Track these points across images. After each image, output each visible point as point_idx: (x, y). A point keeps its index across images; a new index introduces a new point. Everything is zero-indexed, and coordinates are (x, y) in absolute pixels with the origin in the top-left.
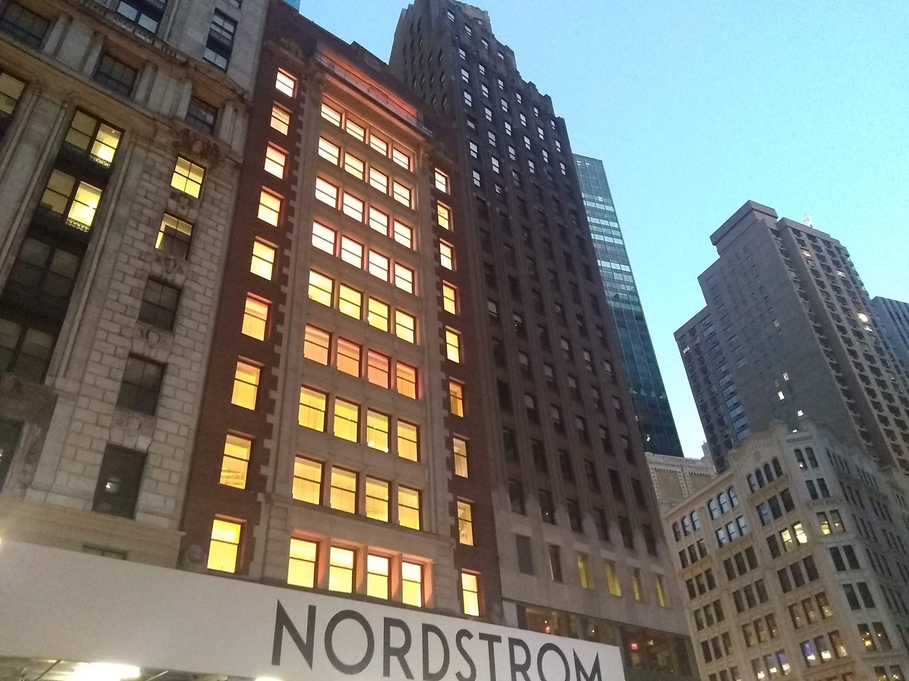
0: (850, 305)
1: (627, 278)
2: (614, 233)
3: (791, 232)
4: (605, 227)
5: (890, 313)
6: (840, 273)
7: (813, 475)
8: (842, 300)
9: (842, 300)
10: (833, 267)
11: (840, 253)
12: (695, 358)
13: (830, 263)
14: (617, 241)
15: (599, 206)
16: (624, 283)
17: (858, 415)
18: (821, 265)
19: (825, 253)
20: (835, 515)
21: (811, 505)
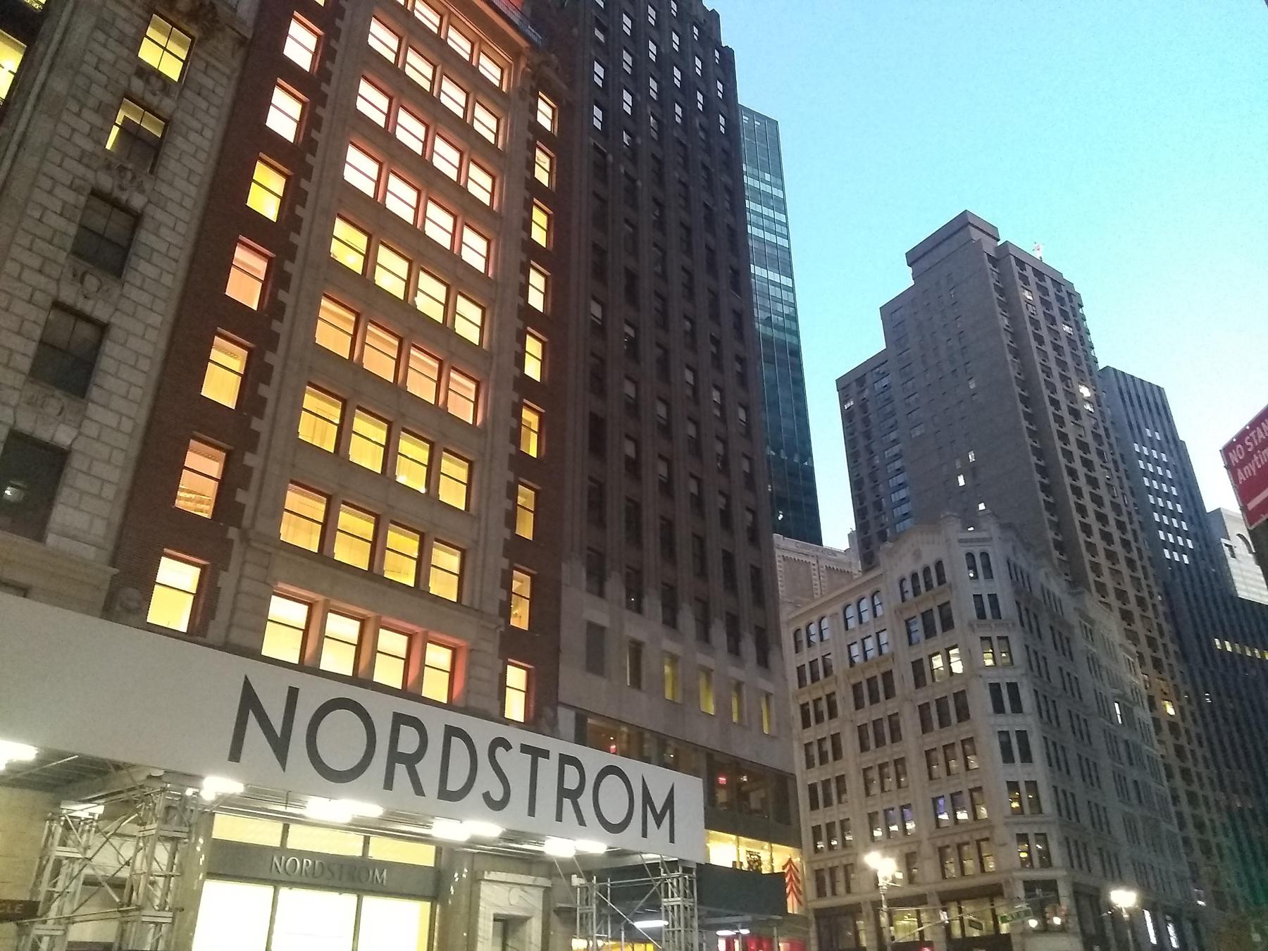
0: (1071, 374)
1: (786, 296)
3: (1013, 262)
4: (768, 218)
5: (1120, 389)
6: (1066, 328)
7: (984, 588)
8: (1062, 364)
9: (1062, 364)
10: (1059, 318)
11: (1071, 301)
12: (858, 417)
13: (1056, 312)
14: (782, 242)
15: (764, 187)
16: (781, 301)
17: (1055, 519)
18: (1044, 313)
19: (1052, 298)
20: (1004, 642)
21: (975, 627)
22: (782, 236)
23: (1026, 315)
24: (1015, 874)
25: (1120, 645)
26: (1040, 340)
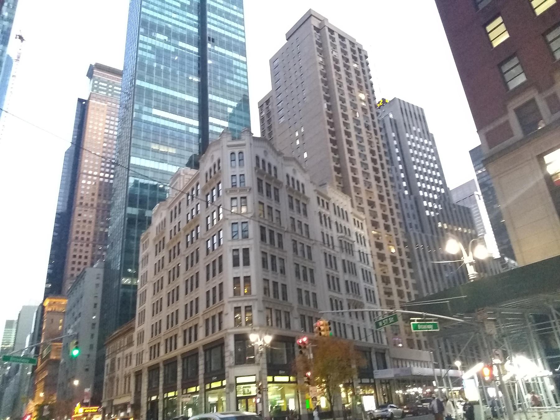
0: (355, 86)
1: (242, 65)
2: (240, 32)
3: (327, 30)
5: (401, 108)
6: (355, 65)
8: (350, 82)
9: (350, 82)
10: (351, 60)
11: (360, 53)
12: (266, 119)
13: (349, 56)
15: (233, 12)
17: (337, 156)
18: (343, 57)
19: (348, 49)
20: (261, 206)
22: (241, 36)
23: (331, 56)
24: (229, 331)
25: (352, 213)
26: (338, 69)
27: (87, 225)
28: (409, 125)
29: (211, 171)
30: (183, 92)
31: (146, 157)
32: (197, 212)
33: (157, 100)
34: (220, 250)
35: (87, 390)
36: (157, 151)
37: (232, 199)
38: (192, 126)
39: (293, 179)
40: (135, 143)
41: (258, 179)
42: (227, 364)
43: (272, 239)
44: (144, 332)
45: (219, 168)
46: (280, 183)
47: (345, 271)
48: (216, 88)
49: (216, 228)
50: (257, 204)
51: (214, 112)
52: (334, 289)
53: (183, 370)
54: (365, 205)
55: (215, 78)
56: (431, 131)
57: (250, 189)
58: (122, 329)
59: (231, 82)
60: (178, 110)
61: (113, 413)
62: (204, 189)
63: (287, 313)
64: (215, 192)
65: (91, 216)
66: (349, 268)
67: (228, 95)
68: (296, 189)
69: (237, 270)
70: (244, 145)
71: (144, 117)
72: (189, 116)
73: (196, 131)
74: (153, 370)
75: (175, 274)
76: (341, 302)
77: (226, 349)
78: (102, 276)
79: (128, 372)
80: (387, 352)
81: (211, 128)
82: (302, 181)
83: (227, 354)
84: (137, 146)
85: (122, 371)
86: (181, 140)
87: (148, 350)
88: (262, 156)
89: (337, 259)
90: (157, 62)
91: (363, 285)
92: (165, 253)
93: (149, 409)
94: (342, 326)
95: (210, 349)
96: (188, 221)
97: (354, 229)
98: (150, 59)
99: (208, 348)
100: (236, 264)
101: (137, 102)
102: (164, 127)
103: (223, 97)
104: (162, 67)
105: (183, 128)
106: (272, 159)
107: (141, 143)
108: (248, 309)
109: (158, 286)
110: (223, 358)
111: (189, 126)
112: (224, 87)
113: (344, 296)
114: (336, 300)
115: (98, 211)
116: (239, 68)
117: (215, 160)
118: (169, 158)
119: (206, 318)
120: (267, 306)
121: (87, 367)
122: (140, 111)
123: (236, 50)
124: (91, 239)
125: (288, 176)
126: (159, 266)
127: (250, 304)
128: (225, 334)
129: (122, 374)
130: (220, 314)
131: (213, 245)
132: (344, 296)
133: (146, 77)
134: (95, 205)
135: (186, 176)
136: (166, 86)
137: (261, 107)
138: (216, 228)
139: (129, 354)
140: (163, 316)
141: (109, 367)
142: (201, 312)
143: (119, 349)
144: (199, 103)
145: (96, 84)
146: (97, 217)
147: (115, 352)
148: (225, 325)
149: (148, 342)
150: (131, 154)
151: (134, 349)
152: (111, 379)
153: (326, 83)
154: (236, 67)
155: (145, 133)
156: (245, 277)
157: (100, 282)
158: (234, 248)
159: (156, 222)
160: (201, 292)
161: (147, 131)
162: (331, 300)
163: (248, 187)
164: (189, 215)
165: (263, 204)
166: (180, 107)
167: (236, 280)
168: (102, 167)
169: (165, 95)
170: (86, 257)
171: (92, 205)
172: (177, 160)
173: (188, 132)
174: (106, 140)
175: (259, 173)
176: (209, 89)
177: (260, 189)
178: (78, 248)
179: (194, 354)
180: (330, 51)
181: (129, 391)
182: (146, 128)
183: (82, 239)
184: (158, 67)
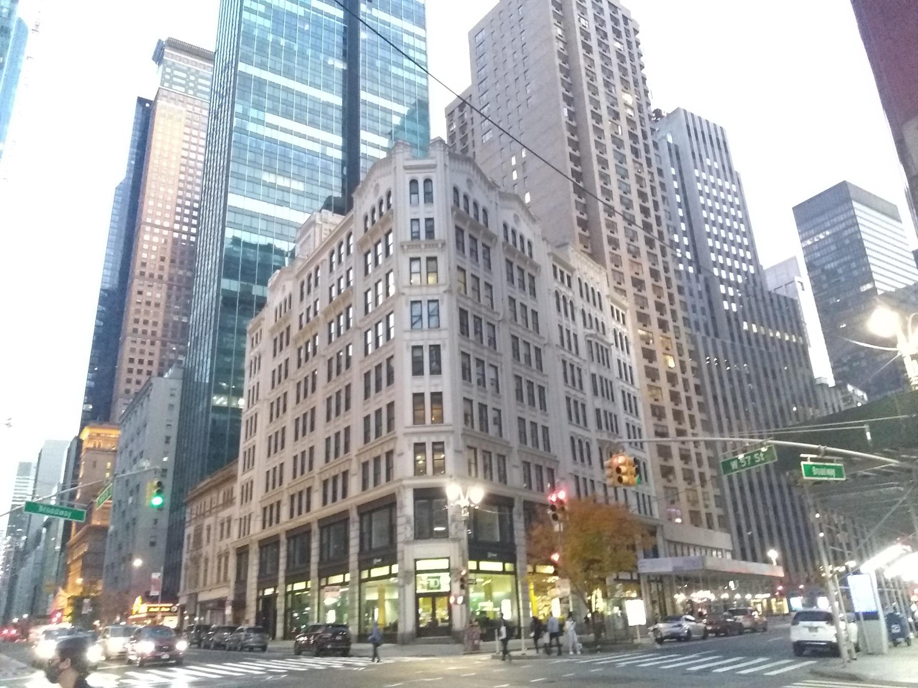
0: (616, 81)
1: (419, 44)
5: (688, 126)
6: (618, 45)
8: (610, 74)
11: (626, 23)
12: (459, 136)
13: (608, 29)
18: (597, 29)
19: (606, 16)
20: (461, 275)
23: (577, 25)
24: (405, 482)
25: (608, 296)
26: (588, 48)
27: (152, 310)
28: (700, 156)
29: (373, 211)
30: (317, 87)
31: (253, 195)
32: (348, 283)
33: (272, 98)
34: (390, 347)
35: (156, 576)
36: (271, 186)
37: (412, 260)
38: (331, 145)
39: (514, 232)
40: (236, 170)
41: (457, 228)
42: (400, 538)
43: (478, 332)
44: (252, 482)
45: (389, 206)
46: (492, 237)
47: (595, 392)
48: (374, 80)
49: (383, 310)
50: (455, 270)
51: (368, 123)
52: (578, 421)
53: (321, 547)
54: (628, 285)
55: (372, 65)
56: (736, 168)
57: (444, 244)
58: (215, 478)
59: (399, 72)
60: (308, 117)
61: (198, 613)
62: (361, 244)
63: (502, 458)
64: (380, 248)
65: (158, 296)
66: (602, 389)
67: (393, 94)
68: (519, 248)
69: (418, 381)
70: (434, 166)
71: (251, 127)
72: (327, 128)
73: (338, 155)
74: (269, 545)
75: (308, 386)
76: (587, 444)
77: (399, 514)
78: (178, 393)
79: (224, 548)
80: (659, 530)
81: (363, 149)
82: (528, 236)
83: (400, 521)
84: (240, 177)
85: (214, 545)
86: (312, 167)
87: (259, 512)
88: (463, 189)
89: (583, 371)
90: (275, 32)
91: (623, 418)
92: (289, 352)
93: (260, 609)
94: (589, 483)
95: (370, 512)
96: (331, 299)
97: (612, 324)
98: (263, 29)
99: (366, 511)
100: (417, 370)
101: (240, 101)
102: (284, 144)
103: (386, 96)
104: (283, 42)
105: (317, 148)
106: (479, 195)
107: (247, 171)
108: (438, 447)
109: (278, 408)
110: (392, 529)
111: (325, 144)
112: (387, 79)
113: (592, 434)
114: (580, 441)
115: (170, 287)
116: (414, 48)
117: (382, 193)
118: (292, 198)
119: (363, 460)
120: (470, 444)
121: (153, 540)
122: (244, 116)
123: (409, 16)
124: (159, 333)
125: (505, 226)
126: (279, 376)
127: (442, 438)
128: (398, 488)
129: (214, 550)
130: (389, 454)
131: (377, 339)
132: (592, 434)
133: (255, 58)
134: (166, 277)
135: (325, 226)
136: (288, 74)
137: (450, 115)
138: (383, 310)
139: (226, 520)
140: (286, 456)
141: (192, 540)
142: (354, 451)
143: (210, 511)
144: (343, 107)
145: (168, 74)
146: (169, 296)
147: (203, 515)
148: (397, 473)
149: (259, 499)
150: (229, 189)
151: (236, 511)
152: (195, 560)
153: (567, 73)
154: (408, 46)
155: (253, 154)
156: (433, 394)
157: (176, 401)
158: (414, 344)
159: (275, 300)
160: (355, 418)
161: (256, 151)
162: (572, 438)
163: (440, 240)
164: (334, 290)
165: (464, 271)
166: (312, 111)
167: (418, 398)
168: (177, 214)
169: (287, 90)
170: (150, 363)
171: (161, 277)
172: (306, 202)
173: (324, 156)
174: (183, 169)
175: (459, 217)
176: (362, 82)
177: (460, 244)
178: (138, 347)
179: (342, 519)
180: (576, 17)
181: (226, 579)
182: (254, 145)
183: (144, 332)
184: (276, 42)
